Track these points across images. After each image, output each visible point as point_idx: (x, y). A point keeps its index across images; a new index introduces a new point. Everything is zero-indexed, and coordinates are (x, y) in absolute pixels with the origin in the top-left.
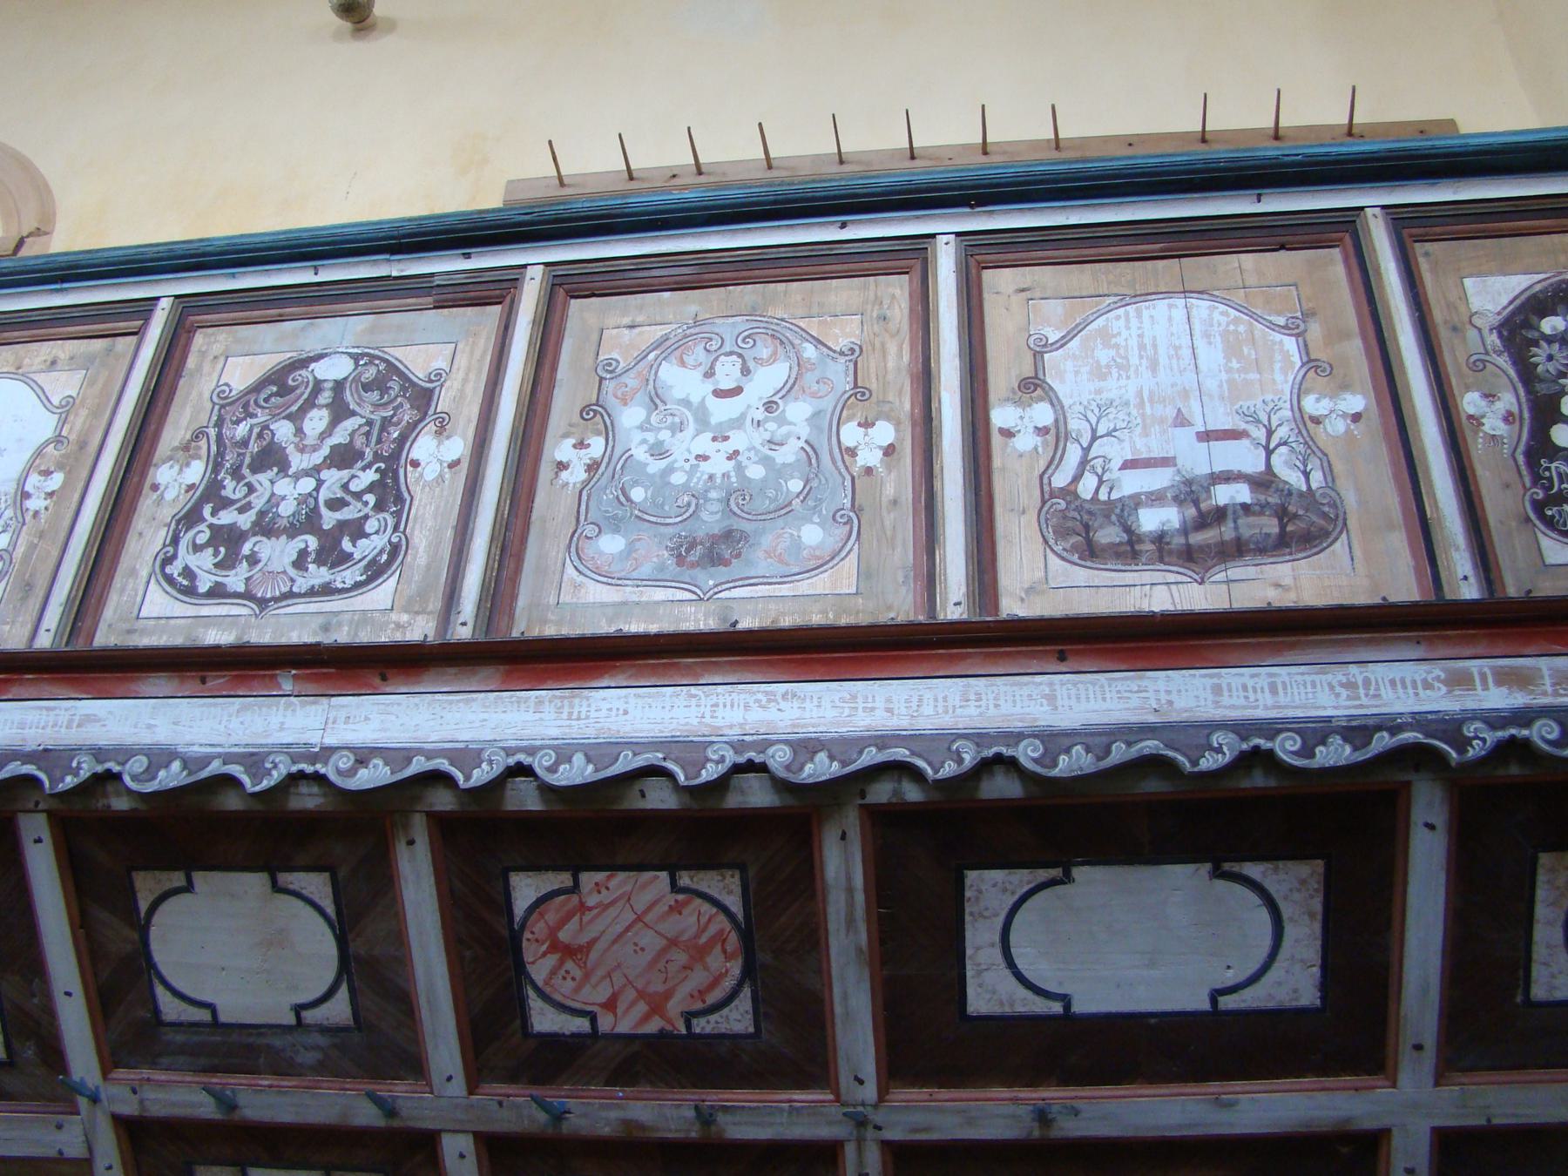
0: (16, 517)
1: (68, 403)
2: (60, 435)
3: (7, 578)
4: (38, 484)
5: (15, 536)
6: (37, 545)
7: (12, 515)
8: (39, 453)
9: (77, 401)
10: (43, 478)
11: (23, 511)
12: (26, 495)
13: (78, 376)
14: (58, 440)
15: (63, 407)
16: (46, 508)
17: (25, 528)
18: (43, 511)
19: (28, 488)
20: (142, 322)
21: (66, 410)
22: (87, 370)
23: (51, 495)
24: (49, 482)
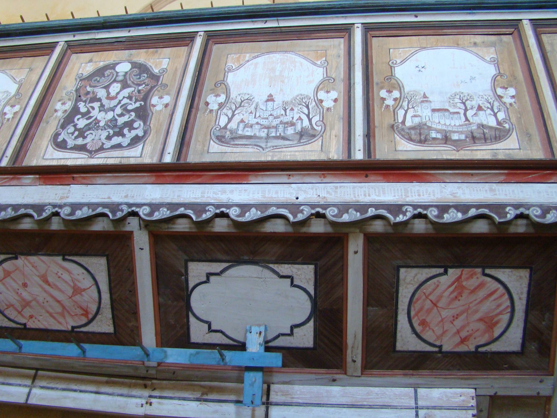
0: (501, 105)
1: (495, 61)
2: (500, 72)
3: (514, 131)
4: (502, 92)
5: (507, 113)
6: (520, 118)
7: (498, 104)
8: (494, 79)
9: (499, 60)
10: (504, 90)
11: (504, 103)
12: (500, 97)
13: (492, 50)
14: (500, 74)
15: (493, 62)
16: (515, 102)
17: (509, 110)
18: (514, 104)
19: (499, 93)
20: (514, 30)
21: (496, 63)
22: (495, 47)
23: (513, 97)
24: (507, 92)
